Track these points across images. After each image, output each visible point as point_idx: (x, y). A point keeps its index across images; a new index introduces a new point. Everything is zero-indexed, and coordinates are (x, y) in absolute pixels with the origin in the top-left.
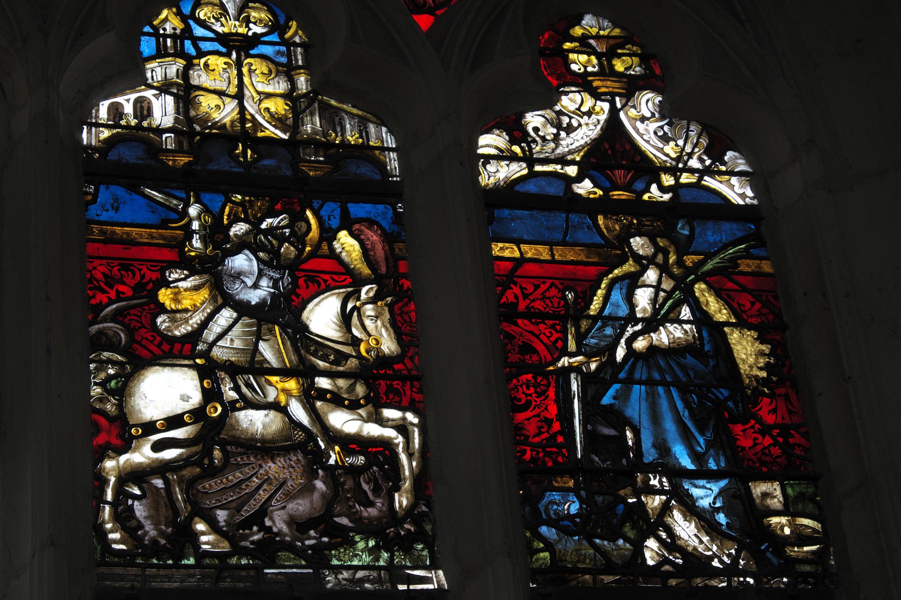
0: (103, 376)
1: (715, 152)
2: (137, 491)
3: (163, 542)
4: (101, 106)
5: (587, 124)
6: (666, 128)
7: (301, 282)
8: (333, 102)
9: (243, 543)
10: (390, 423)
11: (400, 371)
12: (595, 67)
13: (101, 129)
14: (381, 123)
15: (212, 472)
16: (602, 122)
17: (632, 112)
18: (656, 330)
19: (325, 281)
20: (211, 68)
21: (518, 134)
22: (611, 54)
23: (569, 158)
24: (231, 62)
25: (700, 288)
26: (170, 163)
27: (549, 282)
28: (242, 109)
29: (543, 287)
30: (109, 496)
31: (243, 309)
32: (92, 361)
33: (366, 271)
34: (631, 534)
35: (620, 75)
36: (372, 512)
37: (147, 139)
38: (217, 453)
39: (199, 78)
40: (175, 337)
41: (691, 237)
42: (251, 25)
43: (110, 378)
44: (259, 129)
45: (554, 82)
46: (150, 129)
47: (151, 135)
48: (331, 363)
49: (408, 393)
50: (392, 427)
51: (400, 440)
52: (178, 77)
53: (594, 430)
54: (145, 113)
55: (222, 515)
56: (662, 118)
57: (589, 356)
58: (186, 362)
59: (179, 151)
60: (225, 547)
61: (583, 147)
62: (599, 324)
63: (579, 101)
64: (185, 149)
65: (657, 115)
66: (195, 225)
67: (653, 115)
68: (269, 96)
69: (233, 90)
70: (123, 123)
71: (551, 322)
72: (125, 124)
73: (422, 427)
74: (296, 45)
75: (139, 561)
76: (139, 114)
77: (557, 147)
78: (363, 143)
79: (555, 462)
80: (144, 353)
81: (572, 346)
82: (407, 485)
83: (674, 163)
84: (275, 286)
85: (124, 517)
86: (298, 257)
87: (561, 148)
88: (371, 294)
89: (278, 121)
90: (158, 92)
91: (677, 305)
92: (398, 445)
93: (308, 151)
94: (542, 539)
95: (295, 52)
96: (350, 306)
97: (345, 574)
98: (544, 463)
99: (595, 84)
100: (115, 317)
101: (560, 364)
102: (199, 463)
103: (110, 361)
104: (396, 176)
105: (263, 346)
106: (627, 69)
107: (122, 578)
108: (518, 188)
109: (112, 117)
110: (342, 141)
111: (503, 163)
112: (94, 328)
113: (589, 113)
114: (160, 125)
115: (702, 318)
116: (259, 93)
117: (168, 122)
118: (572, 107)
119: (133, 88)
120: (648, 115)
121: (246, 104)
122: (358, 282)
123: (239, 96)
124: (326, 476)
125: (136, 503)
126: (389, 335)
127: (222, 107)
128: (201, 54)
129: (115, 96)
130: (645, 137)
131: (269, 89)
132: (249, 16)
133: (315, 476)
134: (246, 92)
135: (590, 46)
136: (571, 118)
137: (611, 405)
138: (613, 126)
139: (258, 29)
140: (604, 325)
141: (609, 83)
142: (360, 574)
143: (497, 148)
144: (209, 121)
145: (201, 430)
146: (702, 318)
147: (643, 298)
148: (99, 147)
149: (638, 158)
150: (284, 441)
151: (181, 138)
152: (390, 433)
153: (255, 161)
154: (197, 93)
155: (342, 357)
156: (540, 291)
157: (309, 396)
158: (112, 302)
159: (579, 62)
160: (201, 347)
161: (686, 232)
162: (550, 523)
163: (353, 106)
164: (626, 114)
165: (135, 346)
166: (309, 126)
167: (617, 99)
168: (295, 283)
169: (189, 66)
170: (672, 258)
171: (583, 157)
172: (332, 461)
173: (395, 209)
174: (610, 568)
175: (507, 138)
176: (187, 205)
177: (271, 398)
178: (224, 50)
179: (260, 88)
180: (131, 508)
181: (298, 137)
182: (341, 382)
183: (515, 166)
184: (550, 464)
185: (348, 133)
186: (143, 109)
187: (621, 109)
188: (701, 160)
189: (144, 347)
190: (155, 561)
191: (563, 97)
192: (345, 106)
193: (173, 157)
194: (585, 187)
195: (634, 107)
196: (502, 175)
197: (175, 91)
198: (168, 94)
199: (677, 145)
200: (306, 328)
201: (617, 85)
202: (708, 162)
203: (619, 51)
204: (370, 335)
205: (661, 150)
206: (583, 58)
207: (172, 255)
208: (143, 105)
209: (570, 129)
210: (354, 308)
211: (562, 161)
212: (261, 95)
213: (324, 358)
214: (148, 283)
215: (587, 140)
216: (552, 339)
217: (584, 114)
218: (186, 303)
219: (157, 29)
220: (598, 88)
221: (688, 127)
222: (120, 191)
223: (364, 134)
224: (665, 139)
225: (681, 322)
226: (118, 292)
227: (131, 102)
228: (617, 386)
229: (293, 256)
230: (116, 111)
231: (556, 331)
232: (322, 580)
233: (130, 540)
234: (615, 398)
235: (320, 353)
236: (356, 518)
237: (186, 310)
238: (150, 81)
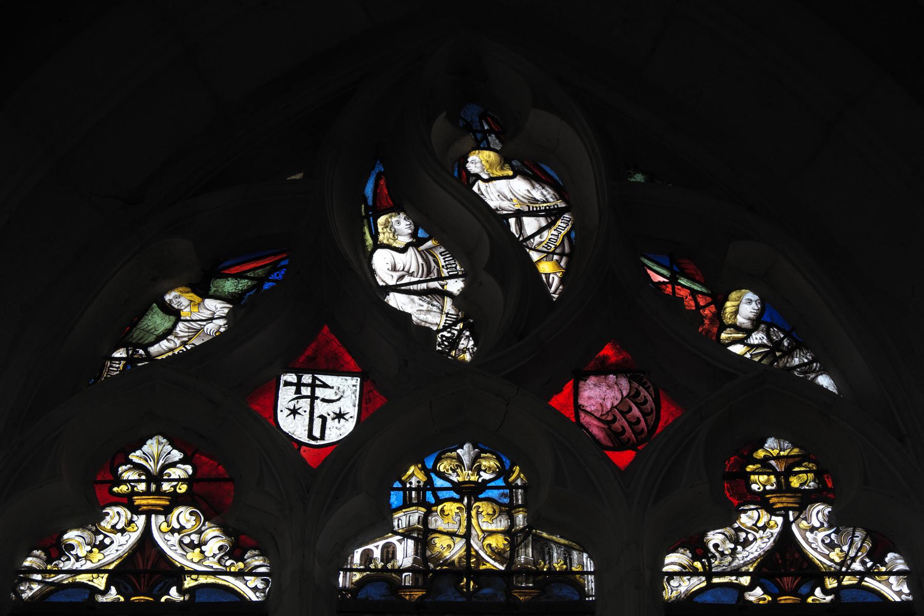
1: (877, 555)
4: (355, 553)
5: (762, 538)
6: (833, 536)
8: (545, 535)
12: (772, 485)
13: (354, 573)
14: (582, 551)
16: (775, 535)
17: (804, 524)
21: (700, 550)
22: (789, 473)
23: (744, 569)
24: (463, 507)
28: (469, 546)
37: (390, 578)
44: (482, 562)
45: (736, 502)
46: (393, 570)
47: (394, 575)
52: (419, 523)
54: (390, 556)
56: (830, 527)
59: (415, 586)
61: (756, 558)
63: (756, 517)
64: (420, 584)
65: (826, 525)
67: (822, 525)
68: (492, 533)
69: (462, 531)
70: (372, 566)
72: (374, 567)
76: (385, 557)
77: (733, 560)
78: (567, 568)
87: (737, 561)
89: (497, 554)
90: (402, 538)
93: (520, 579)
99: (771, 501)
104: (592, 596)
106: (802, 485)
108: (697, 599)
109: (363, 562)
110: (549, 569)
111: (685, 578)
113: (764, 528)
114: (401, 566)
116: (483, 531)
117: (408, 562)
118: (749, 523)
119: (381, 536)
120: (817, 525)
121: (472, 542)
123: (467, 536)
127: (452, 546)
128: (439, 501)
129: (367, 544)
130: (813, 546)
131: (492, 527)
134: (473, 532)
135: (771, 467)
136: (747, 533)
138: (786, 537)
141: (784, 499)
143: (680, 565)
144: (440, 559)
148: (351, 588)
149: (805, 565)
151: (417, 576)
153: (476, 590)
154: (433, 536)
159: (760, 482)
163: (561, 537)
164: (798, 526)
166: (523, 557)
167: (791, 513)
171: (756, 568)
175: (690, 555)
178: (456, 496)
179: (485, 527)
181: (513, 568)
185: (555, 560)
186: (389, 553)
187: (794, 522)
191: (742, 515)
192: (554, 538)
193: (410, 592)
195: (805, 519)
196: (683, 589)
197: (415, 535)
198: (409, 538)
199: (842, 551)
202: (869, 564)
203: (797, 469)
205: (827, 556)
206: (763, 478)
208: (389, 549)
209: (746, 543)
211: (738, 573)
212: (485, 533)
215: (761, 552)
217: (760, 528)
220: (774, 504)
221: (854, 534)
223: (568, 560)
224: (831, 546)
230: (367, 557)
238: (396, 528)
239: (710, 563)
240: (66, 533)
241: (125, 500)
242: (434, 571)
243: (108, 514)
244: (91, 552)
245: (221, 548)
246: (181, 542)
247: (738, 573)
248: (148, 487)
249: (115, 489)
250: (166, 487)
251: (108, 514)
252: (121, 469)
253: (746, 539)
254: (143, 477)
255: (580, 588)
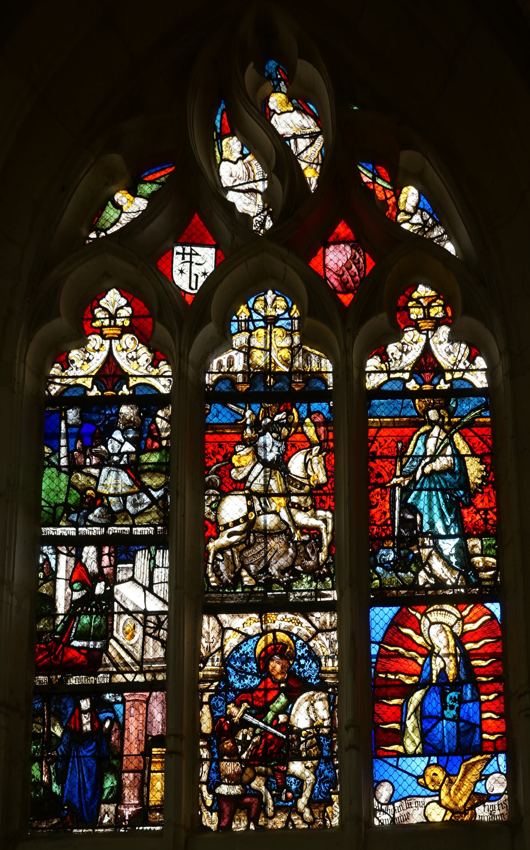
0: (210, 502)
2: (221, 558)
3: (230, 581)
7: (289, 448)
9: (260, 581)
10: (320, 518)
11: (326, 491)
15: (250, 546)
18: (435, 461)
19: (299, 446)
20: (259, 336)
25: (457, 437)
26: (240, 389)
27: (391, 439)
29: (389, 441)
30: (210, 561)
31: (265, 463)
32: (206, 495)
33: (315, 439)
34: (414, 569)
35: (434, 318)
36: (311, 563)
38: (252, 538)
39: (255, 342)
40: (238, 480)
41: (456, 409)
42: (277, 310)
43: (212, 503)
48: (298, 489)
49: (328, 502)
50: (321, 520)
51: (323, 526)
53: (403, 516)
54: (231, 364)
55: (252, 567)
57: (405, 477)
58: (241, 493)
60: (253, 582)
62: (411, 459)
66: (248, 422)
68: (282, 348)
71: (390, 460)
73: (333, 519)
74: (295, 318)
75: (221, 591)
79: (386, 534)
80: (227, 490)
81: (398, 473)
82: (325, 549)
83: (452, 367)
84: (279, 451)
85: (216, 570)
86: (288, 434)
88: (317, 452)
89: (285, 362)
91: (445, 447)
92: (322, 529)
94: (377, 573)
95: (294, 322)
96: (308, 458)
97: (298, 594)
98: (381, 534)
100: (215, 473)
101: (392, 483)
102: (245, 542)
103: (213, 494)
105: (272, 482)
107: (214, 599)
110: (310, 370)
112: (207, 479)
115: (456, 454)
116: (278, 347)
119: (226, 351)
122: (312, 445)
124: (293, 546)
125: (221, 563)
126: (323, 473)
130: (440, 353)
132: (276, 305)
133: (289, 546)
136: (408, 345)
137: (412, 503)
139: (280, 312)
140: (413, 460)
142: (304, 594)
145: (246, 526)
146: (456, 454)
147: (431, 443)
149: (436, 366)
150: (277, 530)
152: (319, 523)
154: (253, 350)
155: (303, 485)
156: (387, 444)
157: (289, 506)
158: (214, 465)
160: (248, 484)
161: (454, 406)
162: (381, 565)
165: (223, 486)
168: (286, 448)
169: (251, 336)
170: (446, 420)
172: (296, 539)
173: (329, 404)
174: (404, 587)
176: (245, 411)
177: (273, 509)
180: (218, 566)
182: (302, 499)
183: (382, 375)
184: (384, 535)
188: (465, 364)
189: (226, 486)
190: (227, 590)
194: (412, 385)
200: (289, 472)
201: (431, 324)
202: (467, 365)
204: (314, 473)
207: (237, 438)
210: (310, 459)
213: (295, 487)
214: (229, 453)
216: (390, 469)
218: (243, 463)
219: (238, 317)
222: (219, 407)
224: (449, 353)
225: (446, 456)
226: (217, 459)
227: (226, 358)
228: (415, 492)
229: (286, 434)
230: (220, 363)
231: (392, 465)
232: (287, 596)
233: (218, 581)
234: (414, 499)
235: (294, 484)
236: (304, 567)
237: (243, 466)
238: (234, 346)
239: (389, 365)
240: (70, 352)
241: (99, 331)
242: (253, 372)
243: (90, 340)
244: (83, 364)
245: (147, 361)
246: (127, 357)
247: (402, 371)
248: (110, 322)
249: (94, 324)
250: (119, 322)
251: (90, 340)
252: (96, 311)
253: (407, 350)
254: (107, 316)
255: (325, 381)
